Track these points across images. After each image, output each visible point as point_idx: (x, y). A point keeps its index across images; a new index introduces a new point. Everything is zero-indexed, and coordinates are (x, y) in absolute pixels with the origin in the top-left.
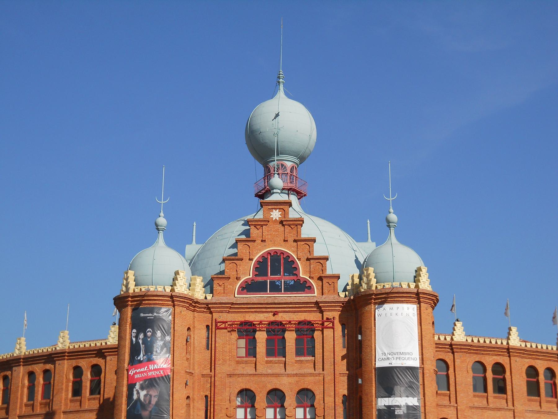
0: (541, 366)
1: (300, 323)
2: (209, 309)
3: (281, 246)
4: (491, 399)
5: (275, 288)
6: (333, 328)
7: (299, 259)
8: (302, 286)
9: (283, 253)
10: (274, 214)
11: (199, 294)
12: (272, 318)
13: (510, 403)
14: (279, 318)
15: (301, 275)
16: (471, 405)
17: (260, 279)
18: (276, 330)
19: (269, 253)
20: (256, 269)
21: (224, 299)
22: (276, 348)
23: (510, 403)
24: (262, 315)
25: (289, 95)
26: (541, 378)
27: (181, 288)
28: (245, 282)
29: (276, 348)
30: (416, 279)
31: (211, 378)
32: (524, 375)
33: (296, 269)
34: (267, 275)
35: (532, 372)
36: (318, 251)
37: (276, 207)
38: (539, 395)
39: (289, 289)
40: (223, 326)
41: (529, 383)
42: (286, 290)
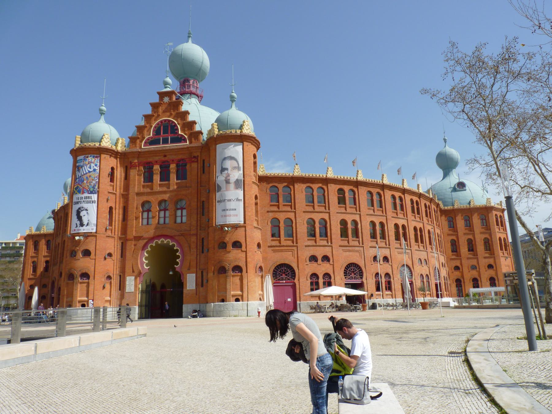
3: (169, 117)
4: (316, 207)
5: (165, 141)
6: (197, 162)
7: (179, 124)
8: (181, 139)
9: (169, 121)
11: (120, 148)
13: (327, 208)
14: (166, 158)
16: (305, 210)
17: (157, 137)
19: (161, 122)
21: (135, 150)
23: (327, 208)
25: (193, 42)
26: (347, 195)
27: (106, 143)
28: (148, 139)
30: (241, 127)
31: (125, 197)
32: (336, 193)
33: (178, 129)
34: (160, 134)
35: (341, 191)
36: (190, 118)
38: (345, 204)
39: (174, 141)
41: (339, 198)
42: (172, 142)
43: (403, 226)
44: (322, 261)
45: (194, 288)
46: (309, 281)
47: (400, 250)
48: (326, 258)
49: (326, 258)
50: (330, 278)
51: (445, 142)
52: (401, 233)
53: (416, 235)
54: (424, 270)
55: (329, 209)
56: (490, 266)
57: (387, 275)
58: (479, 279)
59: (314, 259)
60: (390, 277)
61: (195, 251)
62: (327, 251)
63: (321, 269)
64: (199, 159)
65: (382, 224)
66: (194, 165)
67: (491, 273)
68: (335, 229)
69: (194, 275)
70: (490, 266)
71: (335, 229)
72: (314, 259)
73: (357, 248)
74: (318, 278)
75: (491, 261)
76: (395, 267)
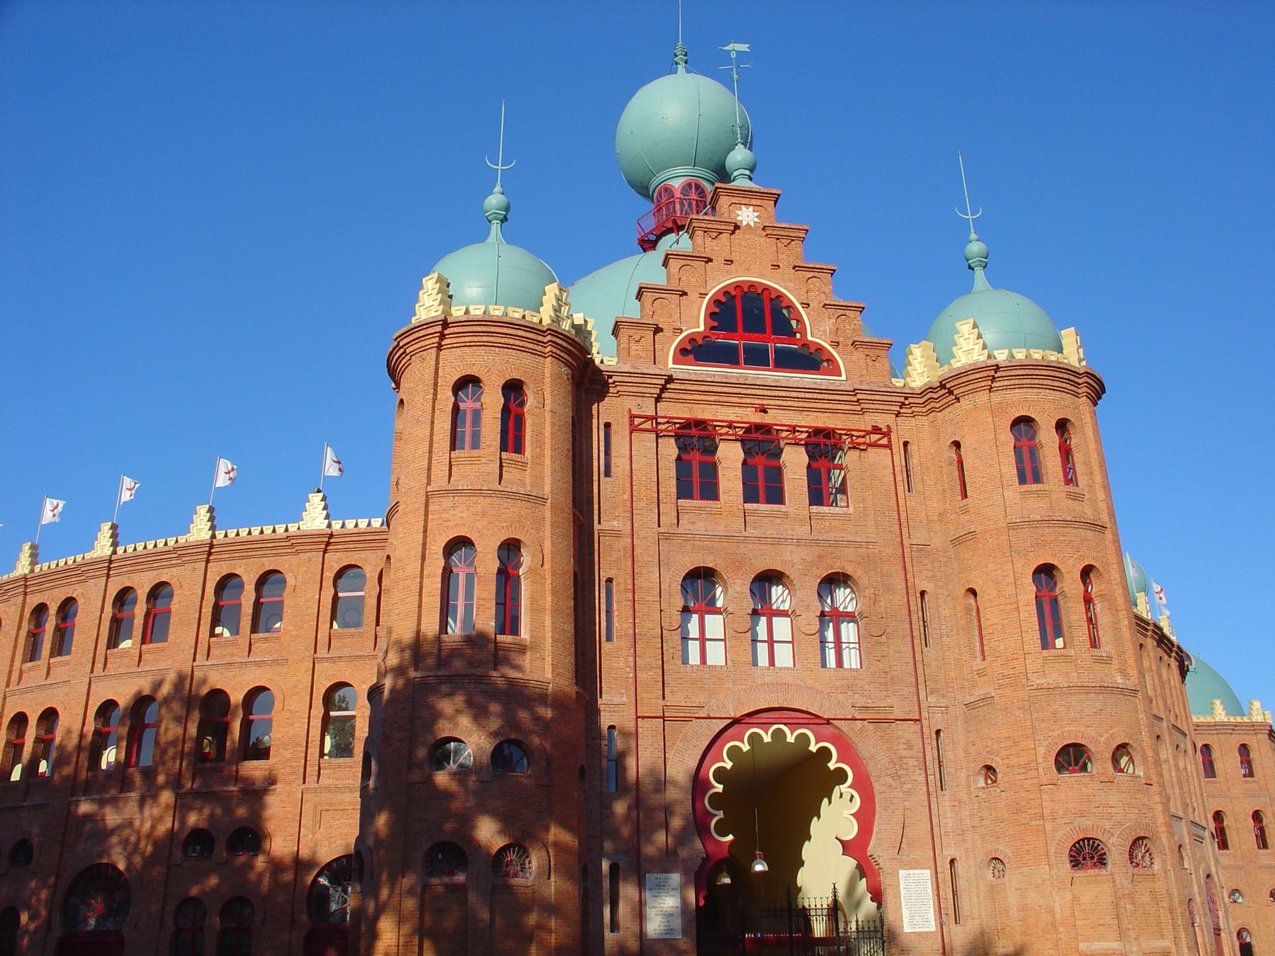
1: (817, 431)
3: (762, 276)
5: (757, 358)
7: (806, 305)
8: (810, 360)
10: (745, 215)
12: (757, 418)
15: (809, 338)
18: (761, 443)
19: (738, 286)
20: (711, 315)
22: (764, 485)
24: (732, 410)
29: (764, 485)
37: (746, 201)
40: (648, 425)
45: (932, 926)
61: (922, 779)
64: (893, 436)
66: (878, 457)
69: (927, 874)
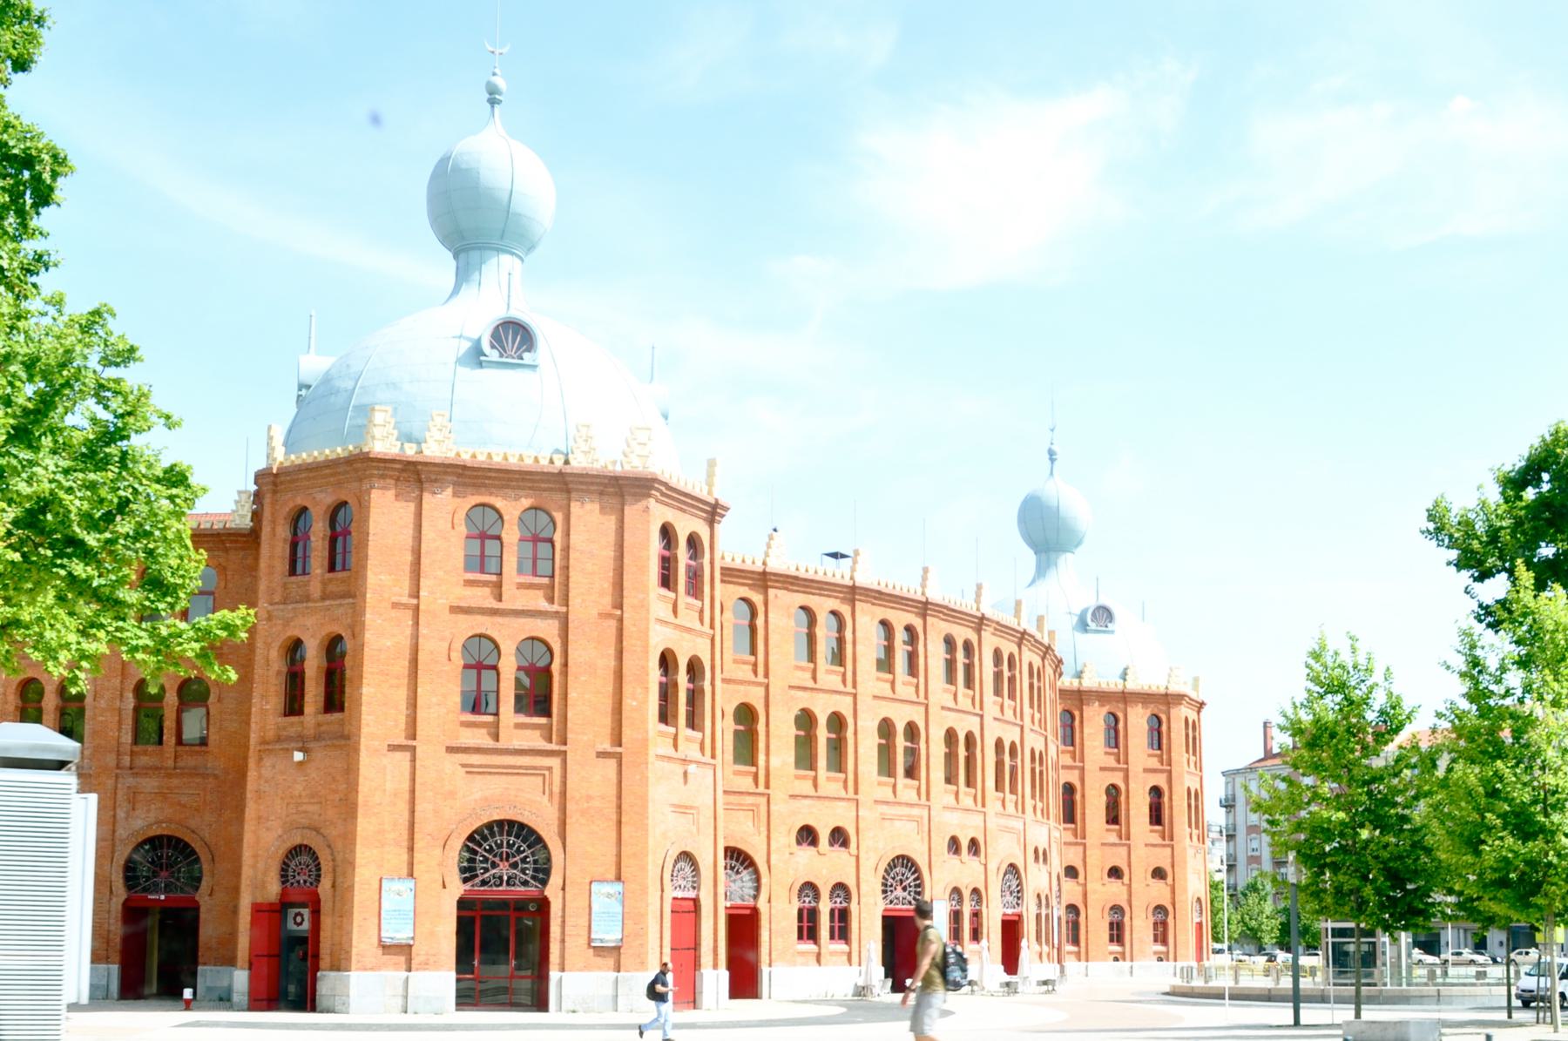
0: (900, 619)
2: (566, 484)
43: (1013, 745)
44: (831, 845)
46: (796, 905)
47: (1003, 821)
48: (839, 837)
49: (839, 837)
50: (848, 897)
51: (1052, 460)
52: (962, 756)
53: (951, 758)
54: (966, 872)
55: (854, 686)
56: (1159, 873)
57: (975, 891)
58: (1127, 909)
59: (807, 835)
60: (979, 901)
62: (842, 816)
63: (826, 866)
65: (969, 738)
67: (1158, 892)
68: (866, 745)
70: (1159, 873)
71: (866, 745)
72: (807, 835)
73: (915, 811)
74: (817, 896)
75: (1162, 858)
76: (992, 867)
